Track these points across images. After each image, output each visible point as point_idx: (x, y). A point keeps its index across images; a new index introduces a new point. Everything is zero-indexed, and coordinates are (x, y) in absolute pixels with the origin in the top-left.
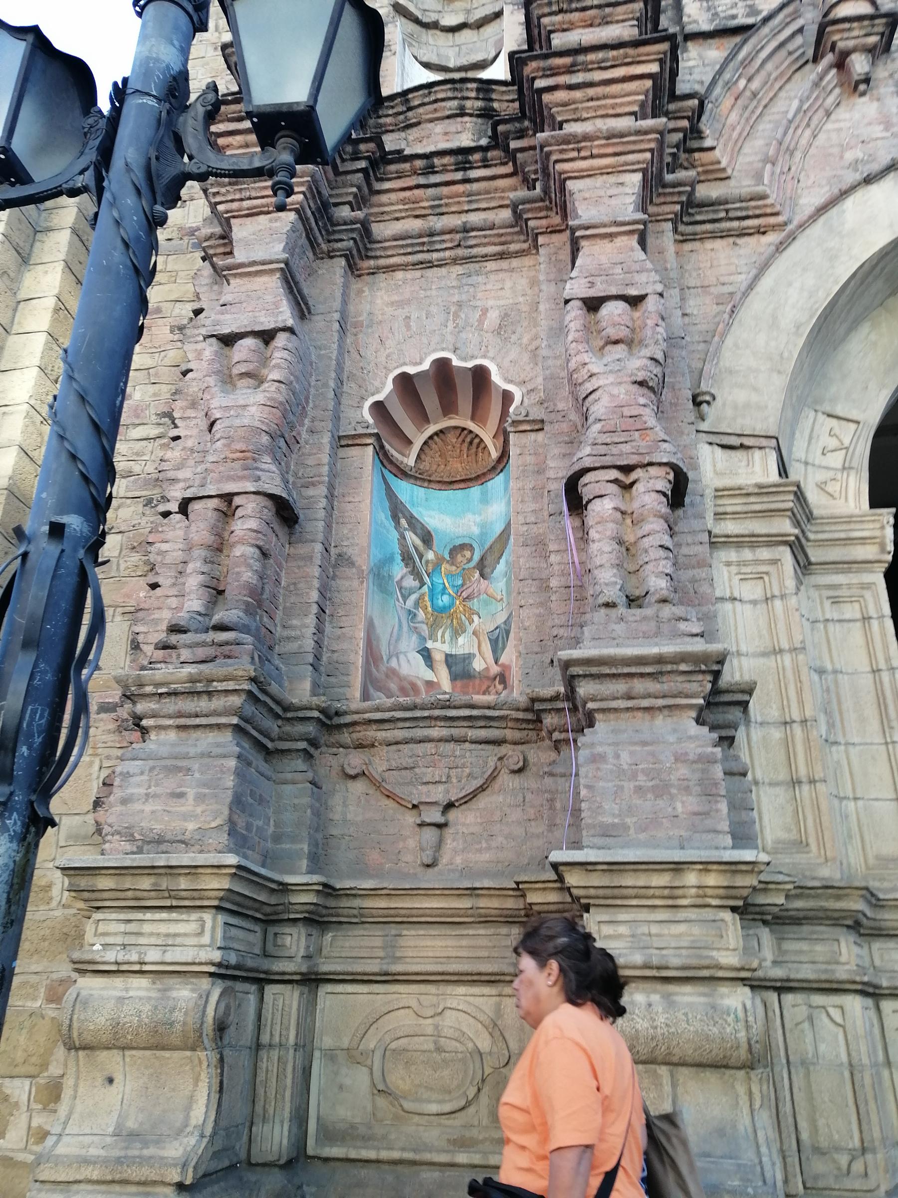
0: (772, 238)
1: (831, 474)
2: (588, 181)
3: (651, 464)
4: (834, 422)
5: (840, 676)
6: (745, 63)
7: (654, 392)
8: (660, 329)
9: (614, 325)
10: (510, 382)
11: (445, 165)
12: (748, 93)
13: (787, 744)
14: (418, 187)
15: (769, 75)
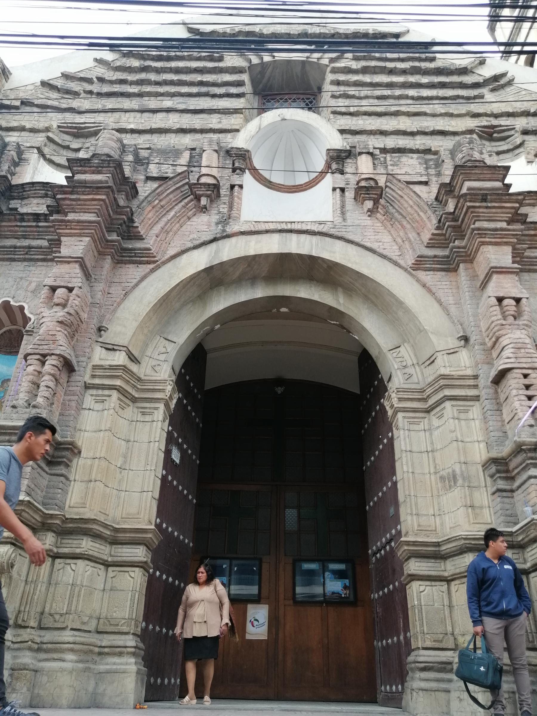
0: (152, 266)
1: (159, 363)
2: (69, 238)
3: (53, 354)
4: (167, 342)
5: (135, 443)
6: (159, 194)
7: (68, 326)
8: (74, 301)
9: (58, 298)
10: (32, 313)
11: (29, 219)
12: (159, 206)
13: (92, 466)
14: (17, 226)
15: (171, 199)
